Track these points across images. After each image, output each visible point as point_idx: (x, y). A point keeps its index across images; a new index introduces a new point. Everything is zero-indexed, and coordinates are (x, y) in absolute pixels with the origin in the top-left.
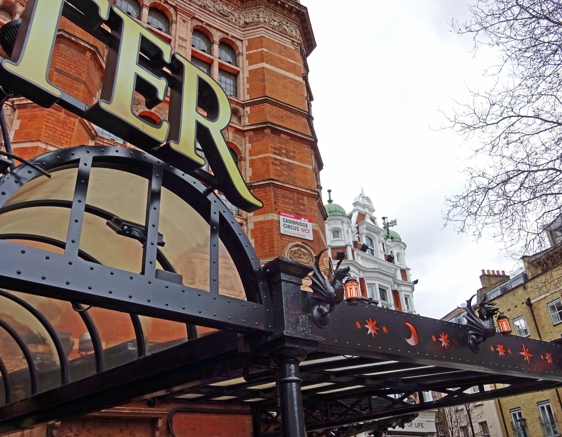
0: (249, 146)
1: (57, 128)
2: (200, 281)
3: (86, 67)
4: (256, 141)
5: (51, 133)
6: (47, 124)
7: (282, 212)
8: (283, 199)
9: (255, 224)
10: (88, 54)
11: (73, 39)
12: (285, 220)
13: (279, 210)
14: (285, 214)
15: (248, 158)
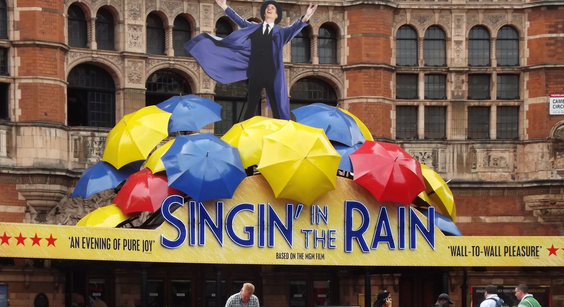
0: (528, 24)
1: (371, 83)
2: (480, 166)
3: (381, 20)
4: (534, 19)
5: (367, 88)
6: (365, 83)
7: (553, 93)
8: (555, 80)
9: (530, 106)
10: (382, 8)
11: (370, 3)
12: (555, 101)
13: (549, 92)
14: (556, 95)
15: (527, 38)
